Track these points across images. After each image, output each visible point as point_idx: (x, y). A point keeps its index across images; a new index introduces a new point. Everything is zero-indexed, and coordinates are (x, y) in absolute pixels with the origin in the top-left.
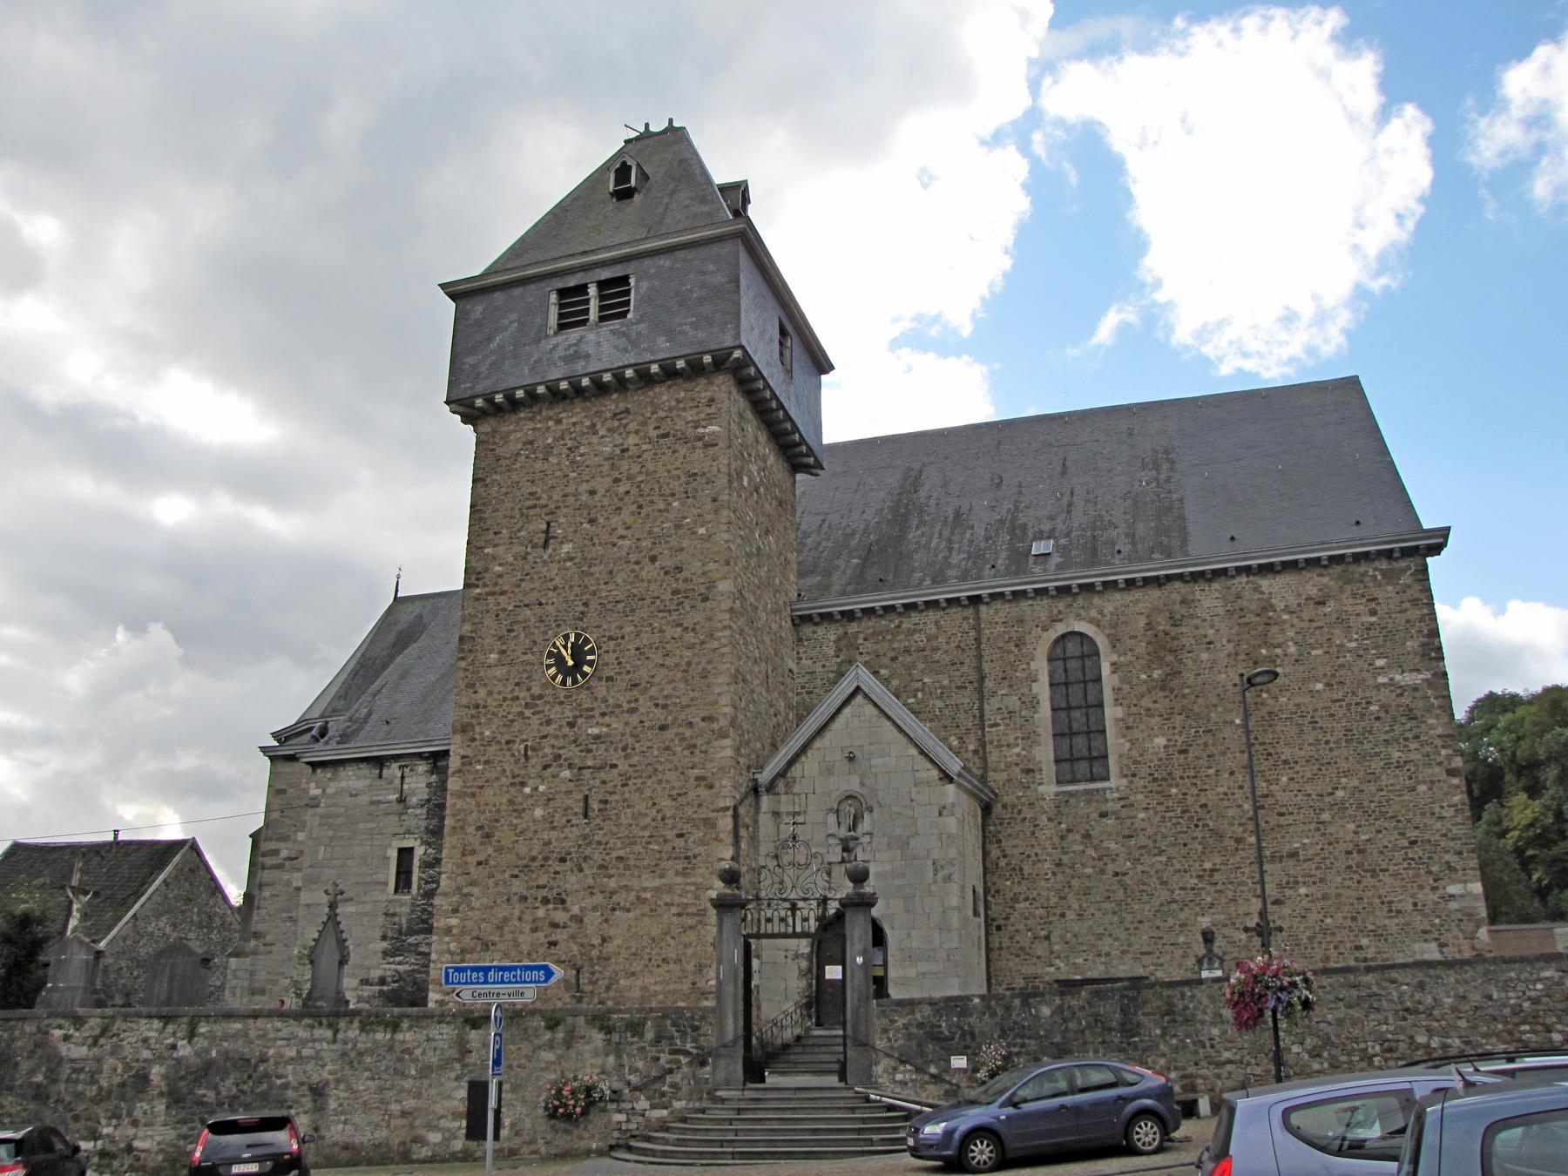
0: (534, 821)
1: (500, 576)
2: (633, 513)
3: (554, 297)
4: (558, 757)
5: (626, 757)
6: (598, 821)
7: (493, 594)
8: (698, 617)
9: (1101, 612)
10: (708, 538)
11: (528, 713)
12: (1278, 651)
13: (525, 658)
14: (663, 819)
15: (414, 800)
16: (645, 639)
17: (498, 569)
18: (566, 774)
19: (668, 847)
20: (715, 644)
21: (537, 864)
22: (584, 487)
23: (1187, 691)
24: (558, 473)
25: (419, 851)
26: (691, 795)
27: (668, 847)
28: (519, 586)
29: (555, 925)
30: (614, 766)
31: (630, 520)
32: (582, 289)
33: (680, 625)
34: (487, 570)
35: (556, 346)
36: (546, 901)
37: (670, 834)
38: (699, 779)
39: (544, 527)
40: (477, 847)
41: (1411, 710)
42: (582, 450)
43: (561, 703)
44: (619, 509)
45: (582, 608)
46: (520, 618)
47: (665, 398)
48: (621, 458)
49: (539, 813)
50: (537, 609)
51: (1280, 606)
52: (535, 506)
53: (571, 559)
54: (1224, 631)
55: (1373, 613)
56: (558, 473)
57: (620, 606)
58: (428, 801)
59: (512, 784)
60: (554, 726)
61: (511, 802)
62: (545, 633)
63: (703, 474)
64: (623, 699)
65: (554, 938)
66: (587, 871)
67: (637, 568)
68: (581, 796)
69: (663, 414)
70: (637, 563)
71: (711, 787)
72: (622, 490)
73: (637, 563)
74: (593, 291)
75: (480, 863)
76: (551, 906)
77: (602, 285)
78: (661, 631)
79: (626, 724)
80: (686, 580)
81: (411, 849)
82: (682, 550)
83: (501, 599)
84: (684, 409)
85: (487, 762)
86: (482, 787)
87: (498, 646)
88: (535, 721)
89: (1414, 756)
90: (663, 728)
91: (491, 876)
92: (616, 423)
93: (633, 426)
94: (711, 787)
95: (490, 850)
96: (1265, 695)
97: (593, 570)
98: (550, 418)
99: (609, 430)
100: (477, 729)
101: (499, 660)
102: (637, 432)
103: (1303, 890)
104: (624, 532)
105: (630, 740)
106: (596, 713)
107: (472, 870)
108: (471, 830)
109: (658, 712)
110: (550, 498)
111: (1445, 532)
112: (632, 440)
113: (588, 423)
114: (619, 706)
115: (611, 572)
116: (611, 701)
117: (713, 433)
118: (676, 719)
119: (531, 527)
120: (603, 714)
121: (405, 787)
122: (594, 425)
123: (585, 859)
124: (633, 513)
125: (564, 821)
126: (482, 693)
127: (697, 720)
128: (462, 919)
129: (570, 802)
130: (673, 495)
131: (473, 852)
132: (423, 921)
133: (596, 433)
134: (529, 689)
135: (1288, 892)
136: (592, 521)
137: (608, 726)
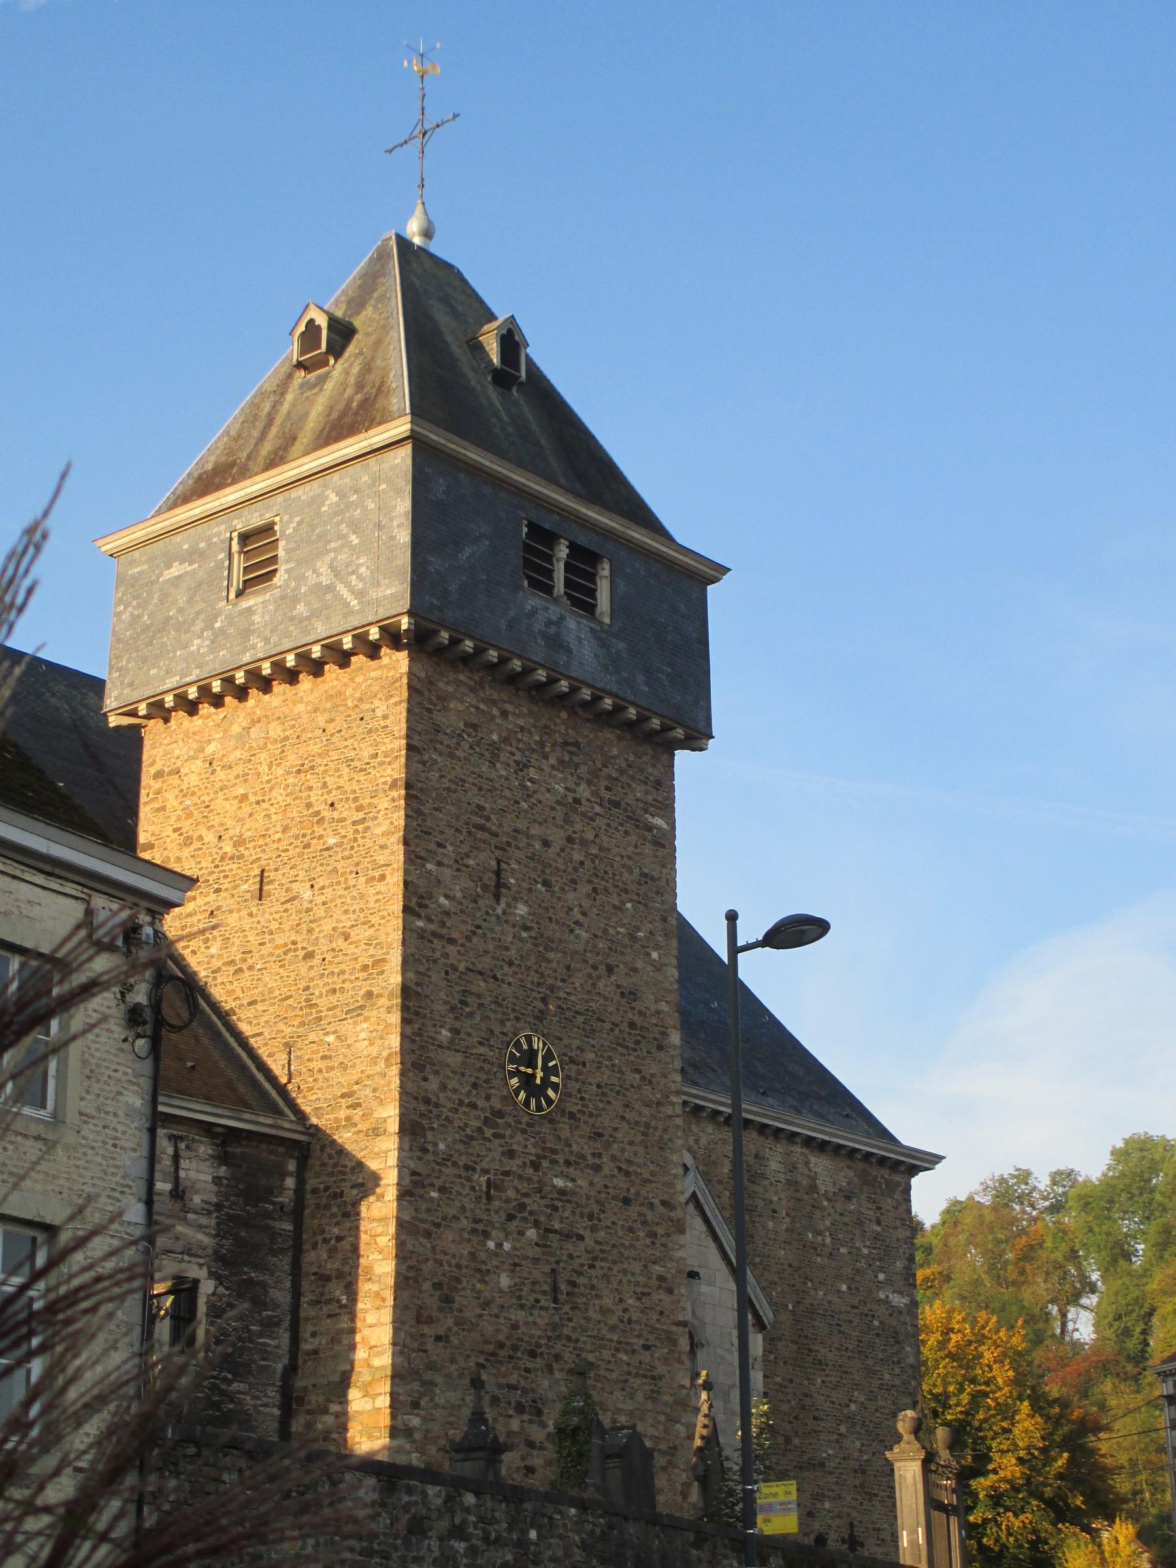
0: (500, 1291)
1: (447, 913)
2: (588, 896)
3: (525, 530)
4: (522, 1207)
5: (594, 1229)
6: (567, 1308)
7: (441, 937)
8: (654, 1069)
9: (697, 1141)
10: (659, 967)
11: (489, 1133)
12: (820, 1238)
13: (482, 1050)
14: (630, 1321)
15: (197, 1199)
16: (605, 1076)
17: (442, 900)
18: (531, 1233)
19: (635, 1361)
20: (669, 1110)
21: (503, 1353)
22: (535, 830)
23: (758, 1260)
24: (507, 793)
25: (207, 1287)
26: (655, 1296)
27: (635, 1361)
28: (468, 938)
29: (531, 1445)
30: (581, 1238)
31: (586, 903)
32: (551, 538)
33: (638, 1071)
34: (430, 897)
35: (533, 612)
36: (520, 1408)
37: (638, 1343)
38: (661, 1278)
39: (494, 863)
40: (435, 1314)
41: (897, 1333)
42: (532, 773)
43: (524, 1132)
44: (574, 881)
45: (540, 1005)
46: (474, 989)
47: (615, 751)
48: (575, 811)
49: (505, 1281)
50: (492, 985)
51: (822, 1189)
52: (481, 828)
53: (527, 929)
54: (784, 1202)
55: (879, 1223)
56: (507, 793)
57: (580, 1019)
58: (219, 1207)
59: (474, 1231)
60: (517, 1162)
61: (473, 1255)
62: (502, 1023)
63: (653, 879)
64: (587, 1151)
65: (529, 1463)
66: (557, 1375)
67: (595, 974)
68: (547, 1269)
69: (614, 774)
70: (595, 968)
71: (670, 1291)
72: (577, 856)
73: (595, 968)
74: (563, 551)
75: (438, 1338)
76: (526, 1417)
77: (572, 546)
78: (621, 1072)
79: (591, 1184)
80: (641, 1013)
81: (196, 1282)
82: (635, 970)
83: (451, 949)
84: (633, 778)
85: (442, 1190)
86: (438, 1225)
87: (449, 1019)
88: (497, 1146)
89: (898, 1383)
90: (626, 1201)
91: (453, 1361)
92: (567, 758)
93: (583, 770)
94: (670, 1291)
95: (450, 1322)
96: (809, 1284)
97: (551, 955)
98: (494, 703)
99: (561, 762)
100: (430, 1136)
101: (452, 1041)
102: (589, 783)
103: (827, 1505)
104: (580, 918)
105: (595, 1208)
106: (561, 1158)
107: (429, 1347)
108: (427, 1286)
109: (621, 1181)
110: (500, 826)
111: (939, 1158)
112: (584, 791)
113: (537, 738)
114: (582, 1157)
115: (568, 968)
116: (575, 1148)
117: (659, 829)
118: (638, 1194)
119: (483, 856)
120: (568, 1163)
121: (182, 1174)
122: (542, 744)
123: (557, 1357)
124: (588, 896)
125: (532, 1299)
126: (434, 1084)
127: (656, 1202)
128: (425, 1420)
129: (537, 1275)
130: (627, 892)
131: (430, 1321)
132: (216, 1406)
133: (546, 757)
134: (488, 1098)
135: (819, 1505)
136: (546, 884)
137: (573, 1180)
